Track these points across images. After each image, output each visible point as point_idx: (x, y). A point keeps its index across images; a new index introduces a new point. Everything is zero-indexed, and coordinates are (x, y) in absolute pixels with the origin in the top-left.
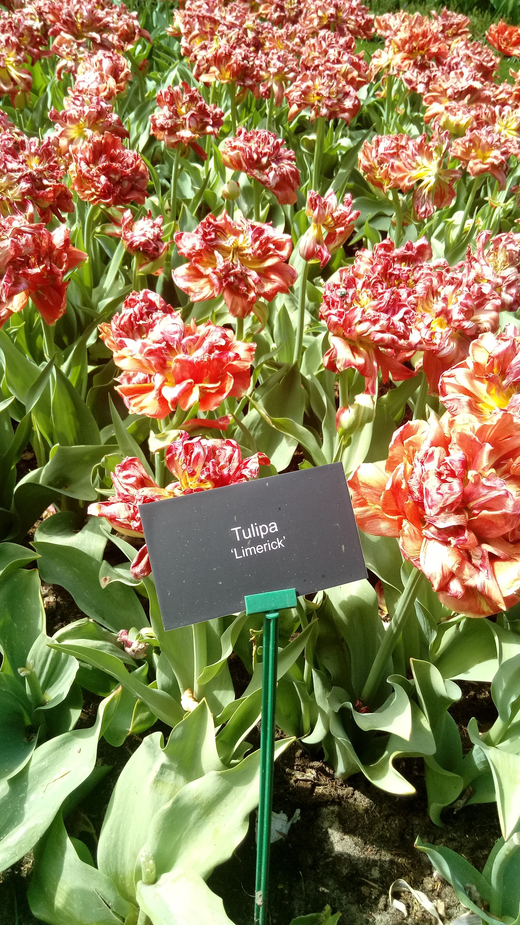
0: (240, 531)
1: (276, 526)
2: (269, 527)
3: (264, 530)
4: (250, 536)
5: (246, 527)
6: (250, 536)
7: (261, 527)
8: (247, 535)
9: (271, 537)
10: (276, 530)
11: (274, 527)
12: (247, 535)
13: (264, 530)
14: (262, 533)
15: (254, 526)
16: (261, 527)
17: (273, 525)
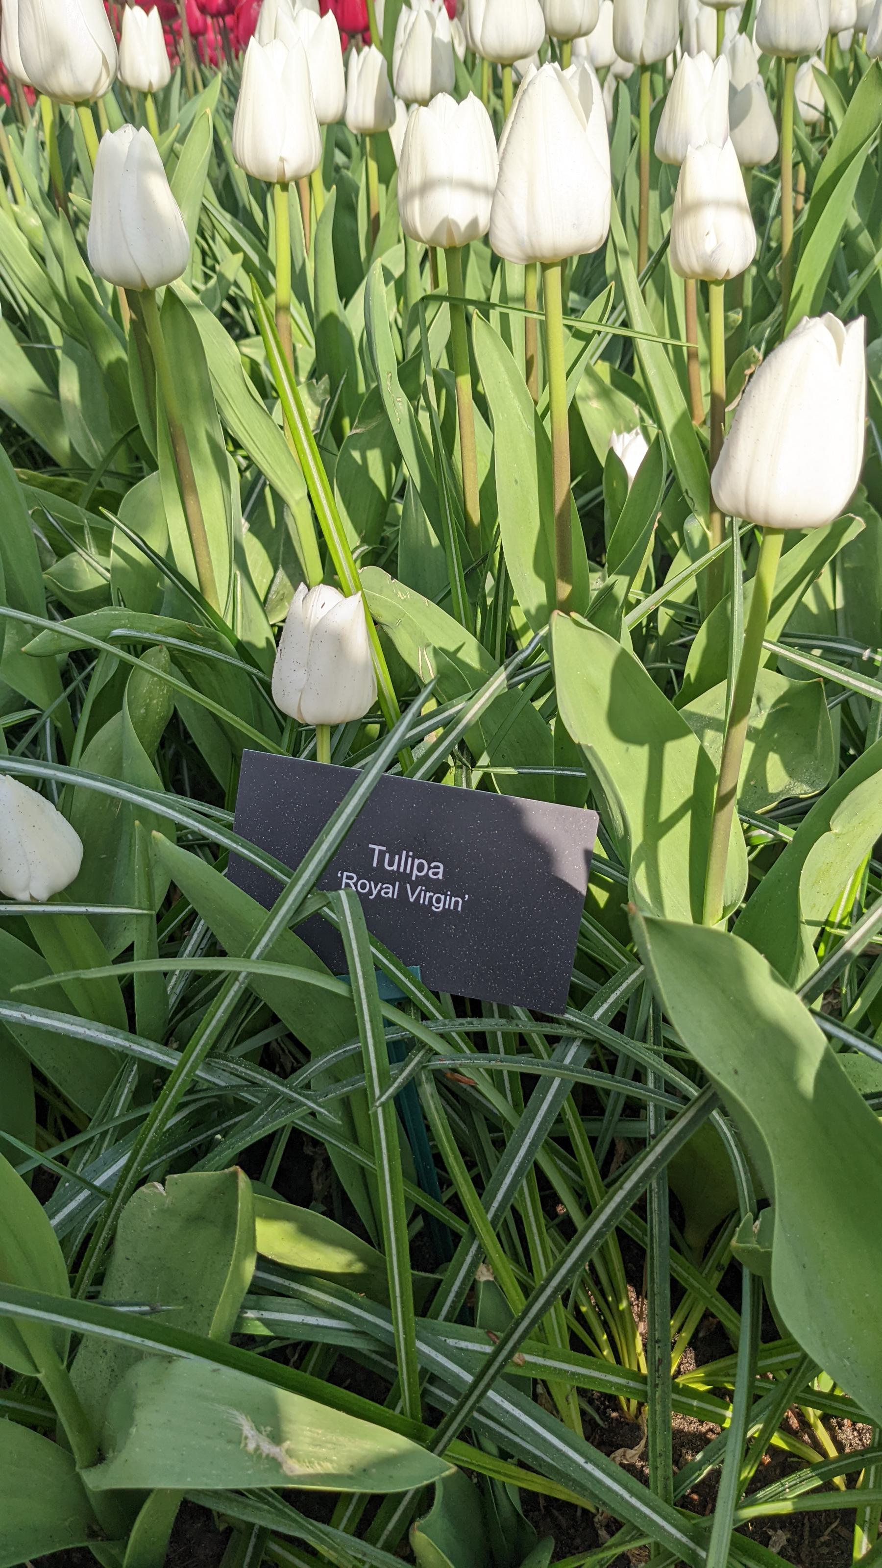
0: (382, 854)
1: (441, 870)
2: (430, 868)
3: (420, 868)
4: (395, 868)
5: (394, 851)
6: (395, 868)
7: (417, 862)
8: (391, 864)
9: (426, 882)
10: (440, 876)
11: (438, 872)
12: (391, 864)
13: (420, 868)
14: (415, 871)
15: (407, 856)
16: (417, 862)
17: (438, 867)
